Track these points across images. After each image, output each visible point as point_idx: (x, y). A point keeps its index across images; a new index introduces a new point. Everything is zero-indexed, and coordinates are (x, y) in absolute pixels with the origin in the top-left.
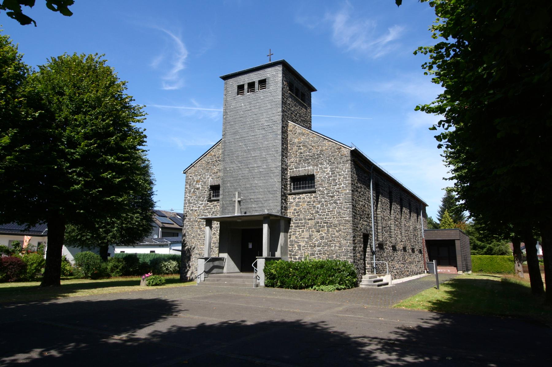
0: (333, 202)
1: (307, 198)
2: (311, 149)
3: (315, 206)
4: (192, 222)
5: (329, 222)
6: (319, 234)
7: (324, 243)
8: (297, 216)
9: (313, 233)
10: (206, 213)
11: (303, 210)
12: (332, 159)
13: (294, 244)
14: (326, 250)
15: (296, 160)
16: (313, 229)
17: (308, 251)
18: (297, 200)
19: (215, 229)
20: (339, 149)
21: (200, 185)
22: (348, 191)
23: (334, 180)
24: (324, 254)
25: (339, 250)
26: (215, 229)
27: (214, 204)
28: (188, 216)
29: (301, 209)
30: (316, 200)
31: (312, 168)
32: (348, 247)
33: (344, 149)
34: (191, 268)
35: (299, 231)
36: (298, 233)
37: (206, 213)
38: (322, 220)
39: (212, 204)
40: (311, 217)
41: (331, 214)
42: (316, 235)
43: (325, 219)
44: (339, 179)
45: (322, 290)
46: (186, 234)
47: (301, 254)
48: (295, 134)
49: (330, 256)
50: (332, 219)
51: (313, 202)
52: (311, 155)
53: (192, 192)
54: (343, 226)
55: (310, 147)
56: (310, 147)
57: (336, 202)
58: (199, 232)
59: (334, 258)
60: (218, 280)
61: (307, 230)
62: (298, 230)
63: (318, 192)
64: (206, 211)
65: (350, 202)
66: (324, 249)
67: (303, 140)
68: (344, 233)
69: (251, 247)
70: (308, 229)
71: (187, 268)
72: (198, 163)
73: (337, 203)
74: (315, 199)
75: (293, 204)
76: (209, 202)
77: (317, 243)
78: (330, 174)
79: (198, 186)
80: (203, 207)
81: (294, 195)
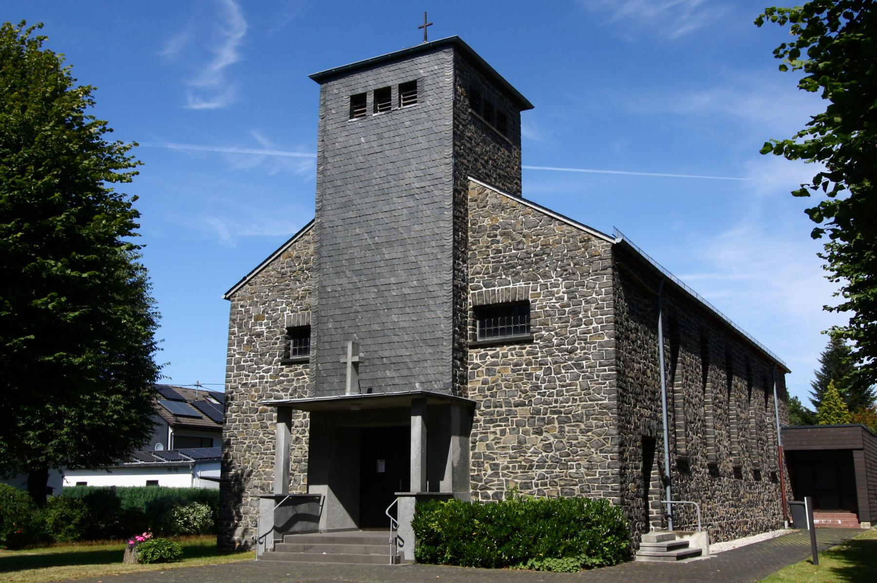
0: (573, 364)
1: (512, 355)
2: (521, 240)
3: (531, 374)
4: (246, 413)
5: (562, 410)
6: (540, 438)
7: (553, 459)
8: (489, 398)
9: (527, 437)
10: (278, 391)
11: (503, 384)
12: (569, 265)
13: (483, 463)
14: (557, 476)
15: (487, 268)
16: (527, 427)
17: (516, 478)
18: (489, 360)
19: (300, 429)
20: (585, 241)
21: (263, 327)
22: (606, 339)
23: (575, 313)
24: (554, 484)
25: (587, 475)
26: (300, 429)
27: (296, 370)
28: (235, 398)
29: (500, 382)
30: (533, 360)
31: (523, 285)
32: (609, 468)
33: (596, 242)
34: (243, 521)
35: (495, 433)
36: (491, 437)
37: (278, 391)
38: (547, 406)
39: (291, 371)
40: (521, 399)
41: (567, 391)
42: (535, 442)
43: (554, 405)
44: (586, 311)
45: (550, 569)
46: (232, 442)
47: (499, 485)
48: (485, 207)
49: (566, 490)
50: (570, 404)
51: (526, 365)
52: (522, 256)
53: (245, 342)
54: (596, 419)
55: (519, 238)
56: (519, 238)
57: (579, 364)
58: (261, 435)
59: (577, 493)
60: (305, 549)
61: (514, 429)
62: (492, 430)
63: (539, 341)
64: (278, 387)
65: (612, 364)
66: (553, 472)
67: (501, 221)
68: (600, 435)
69: (384, 471)
70: (514, 426)
71: (233, 520)
72: (259, 275)
73: (583, 367)
74: (531, 357)
75: (480, 369)
76: (284, 367)
77: (536, 459)
78: (566, 299)
79: (258, 329)
80: (271, 377)
81: (481, 348)
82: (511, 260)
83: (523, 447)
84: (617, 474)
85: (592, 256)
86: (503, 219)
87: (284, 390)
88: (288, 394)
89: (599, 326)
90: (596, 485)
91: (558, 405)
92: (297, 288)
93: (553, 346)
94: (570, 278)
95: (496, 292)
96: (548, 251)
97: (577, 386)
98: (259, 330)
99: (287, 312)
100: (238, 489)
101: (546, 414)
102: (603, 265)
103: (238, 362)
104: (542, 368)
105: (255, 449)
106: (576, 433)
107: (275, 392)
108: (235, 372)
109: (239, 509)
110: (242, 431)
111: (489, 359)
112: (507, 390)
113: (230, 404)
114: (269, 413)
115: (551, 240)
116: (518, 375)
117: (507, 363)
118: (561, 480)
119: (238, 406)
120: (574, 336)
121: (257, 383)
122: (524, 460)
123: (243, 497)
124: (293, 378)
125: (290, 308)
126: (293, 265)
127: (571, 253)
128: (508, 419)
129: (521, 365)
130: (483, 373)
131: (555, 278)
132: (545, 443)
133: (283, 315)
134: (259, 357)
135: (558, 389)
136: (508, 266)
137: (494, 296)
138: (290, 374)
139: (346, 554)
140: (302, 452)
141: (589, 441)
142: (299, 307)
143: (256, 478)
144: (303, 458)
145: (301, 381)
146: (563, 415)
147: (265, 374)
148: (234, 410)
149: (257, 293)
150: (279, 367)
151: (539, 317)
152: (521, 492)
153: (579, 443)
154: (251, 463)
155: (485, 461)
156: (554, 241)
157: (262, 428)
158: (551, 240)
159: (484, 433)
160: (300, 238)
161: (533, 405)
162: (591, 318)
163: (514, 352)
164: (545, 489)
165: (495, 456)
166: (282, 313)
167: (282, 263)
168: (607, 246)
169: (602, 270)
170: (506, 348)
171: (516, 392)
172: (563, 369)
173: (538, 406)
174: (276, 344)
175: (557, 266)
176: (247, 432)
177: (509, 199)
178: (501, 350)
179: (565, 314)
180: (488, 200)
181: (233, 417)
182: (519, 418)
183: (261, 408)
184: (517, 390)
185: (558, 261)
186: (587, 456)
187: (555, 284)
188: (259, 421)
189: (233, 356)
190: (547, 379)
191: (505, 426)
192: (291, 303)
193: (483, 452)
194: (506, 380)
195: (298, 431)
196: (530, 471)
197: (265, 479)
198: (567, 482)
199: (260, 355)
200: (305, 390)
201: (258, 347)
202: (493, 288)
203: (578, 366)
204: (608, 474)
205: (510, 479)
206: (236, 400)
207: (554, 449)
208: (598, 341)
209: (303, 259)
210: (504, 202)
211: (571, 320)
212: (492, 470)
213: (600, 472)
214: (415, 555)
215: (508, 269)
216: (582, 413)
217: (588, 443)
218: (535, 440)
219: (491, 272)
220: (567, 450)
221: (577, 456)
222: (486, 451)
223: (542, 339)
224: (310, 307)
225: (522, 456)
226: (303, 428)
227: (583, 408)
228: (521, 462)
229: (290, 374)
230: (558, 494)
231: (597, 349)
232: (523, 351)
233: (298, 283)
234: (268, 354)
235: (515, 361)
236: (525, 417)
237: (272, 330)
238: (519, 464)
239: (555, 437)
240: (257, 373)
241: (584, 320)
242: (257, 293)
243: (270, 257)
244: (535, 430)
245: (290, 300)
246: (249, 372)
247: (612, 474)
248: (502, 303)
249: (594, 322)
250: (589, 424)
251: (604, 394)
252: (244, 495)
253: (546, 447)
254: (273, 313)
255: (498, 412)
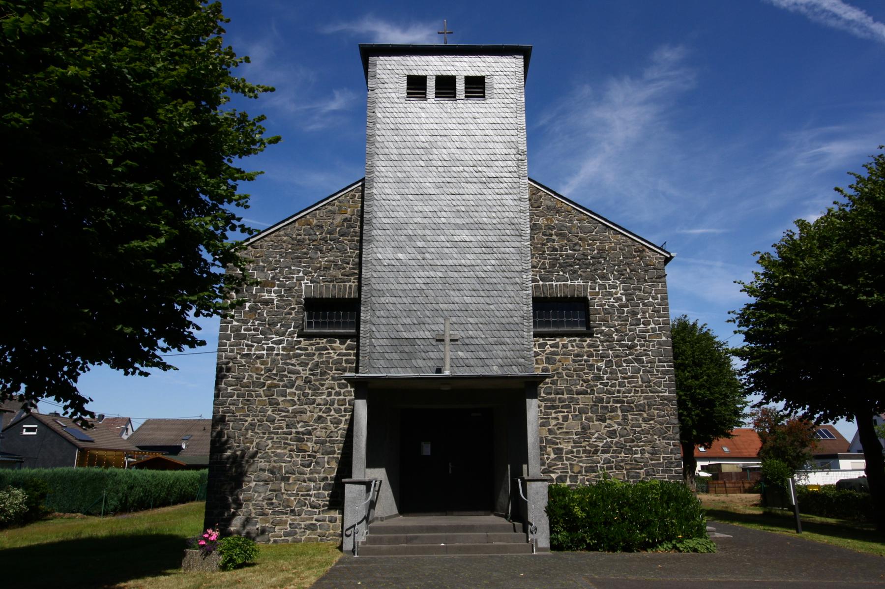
0: (634, 359)
1: (572, 346)
2: (578, 243)
3: (593, 365)
4: (248, 387)
5: (625, 399)
6: (604, 424)
7: (618, 445)
8: (550, 385)
9: (591, 424)
10: (293, 365)
11: (564, 372)
12: (626, 270)
13: (545, 447)
14: (622, 461)
15: (544, 264)
16: (590, 414)
17: (581, 462)
18: (548, 349)
19: (324, 408)
20: (639, 251)
21: (273, 294)
22: (664, 338)
23: (634, 313)
24: (619, 468)
25: (652, 460)
26: (324, 408)
27: (318, 343)
28: (233, 370)
29: (560, 370)
30: (594, 353)
31: (581, 283)
32: (671, 453)
33: (650, 253)
34: (244, 509)
35: (557, 418)
36: (553, 422)
37: (293, 365)
38: (609, 396)
39: (311, 345)
40: (584, 388)
41: (629, 382)
42: (599, 429)
43: (616, 394)
44: (644, 312)
45: (695, 550)
46: (227, 419)
47: (563, 468)
48: (539, 207)
49: (633, 474)
50: (632, 394)
51: (588, 356)
52: (579, 257)
53: (247, 309)
54: (657, 409)
55: (576, 240)
56: (576, 240)
57: (640, 359)
58: (269, 413)
59: (642, 476)
60: (408, 540)
61: (576, 416)
62: (554, 415)
63: (599, 335)
64: (294, 361)
65: (670, 361)
66: (618, 457)
67: (557, 222)
68: (661, 424)
69: (429, 454)
70: (577, 413)
71: (229, 508)
72: (266, 239)
73: (643, 362)
74: (592, 350)
75: (539, 357)
76: (302, 339)
77: (601, 444)
78: (624, 299)
79: (266, 296)
80: (284, 349)
81: (540, 337)
82: (568, 259)
83: (587, 433)
84: (680, 459)
85: (647, 265)
86: (558, 220)
87: (302, 365)
88: (307, 369)
89: (657, 326)
90: (661, 469)
91: (621, 395)
92: (318, 258)
93: (614, 341)
94: (627, 282)
95: (554, 287)
96: (604, 255)
97: (638, 379)
98: (266, 297)
99: (306, 281)
100: (236, 472)
101: (609, 403)
102: (658, 274)
103: (237, 330)
104: (603, 360)
105: (260, 428)
106: (639, 421)
107: (290, 366)
108: (232, 340)
109: (237, 495)
110: (242, 407)
111: (548, 348)
112: (569, 378)
113: (225, 376)
114: (281, 388)
115: (607, 247)
116: (579, 365)
117: (568, 354)
118: (627, 464)
119: (237, 378)
120: (633, 334)
121: (264, 355)
122: (588, 445)
123: (244, 481)
124: (313, 352)
125: (310, 278)
126: (312, 233)
127: (627, 260)
128: (571, 406)
129: (583, 356)
130: (543, 361)
131: (612, 280)
132: (609, 429)
133: (300, 284)
134: (267, 326)
135: (620, 380)
136: (565, 265)
137: (551, 291)
138: (310, 348)
139: (461, 544)
140: (326, 432)
141: (651, 429)
142: (321, 278)
143: (263, 460)
144: (328, 439)
145: (324, 356)
146: (626, 404)
147: (276, 346)
148: (230, 383)
149: (264, 258)
150: (295, 339)
151: (599, 314)
152: (586, 476)
153: (642, 430)
154: (254, 443)
155: (548, 446)
156: (610, 248)
157: (270, 405)
158: (607, 247)
159: (545, 418)
160: (322, 206)
161: (596, 394)
162: (649, 319)
163: (574, 344)
164: (610, 472)
165: (558, 441)
166: (298, 282)
167: (298, 230)
168: (660, 258)
169: (656, 278)
170: (566, 340)
171: (578, 381)
172: (624, 362)
173: (601, 395)
174: (291, 314)
175: (614, 270)
176: (249, 409)
177: (563, 204)
178: (561, 341)
179: (624, 314)
180: (542, 202)
181: (229, 391)
182: (581, 406)
183: (269, 382)
184: (579, 379)
185: (615, 266)
186: (651, 442)
187: (613, 285)
188: (266, 397)
189: (229, 323)
190: (609, 371)
191: (567, 412)
192: (311, 273)
193: (545, 437)
194: (568, 369)
195: (320, 410)
196: (595, 455)
197: (275, 461)
198: (633, 466)
199: (269, 324)
200: (331, 365)
201: (265, 315)
202: (550, 283)
203: (640, 361)
204: (671, 459)
205: (575, 462)
206: (235, 373)
207: (618, 435)
208: (656, 340)
209: (326, 229)
210: (559, 206)
211: (630, 319)
212: (555, 454)
213: (663, 457)
214: (551, 543)
215: (566, 267)
216: (644, 403)
217: (651, 430)
218: (599, 426)
219: (548, 267)
220: (631, 437)
221: (641, 442)
222: (548, 435)
223: (603, 334)
224: (336, 279)
225: (586, 441)
226: (328, 406)
227: (644, 399)
228: (585, 447)
229: (310, 348)
230: (624, 477)
231: (656, 347)
232: (584, 343)
233: (319, 253)
234: (279, 324)
235: (576, 352)
236: (588, 405)
237: (284, 298)
238: (584, 448)
239: (619, 424)
240: (263, 344)
241: (642, 320)
242: (264, 258)
243: (283, 222)
244: (599, 417)
245: (310, 269)
246: (252, 341)
247: (675, 459)
248: (561, 297)
249: (652, 323)
250: (651, 414)
251: (664, 387)
252: (246, 479)
253: (610, 433)
254: (286, 281)
255: (559, 399)
